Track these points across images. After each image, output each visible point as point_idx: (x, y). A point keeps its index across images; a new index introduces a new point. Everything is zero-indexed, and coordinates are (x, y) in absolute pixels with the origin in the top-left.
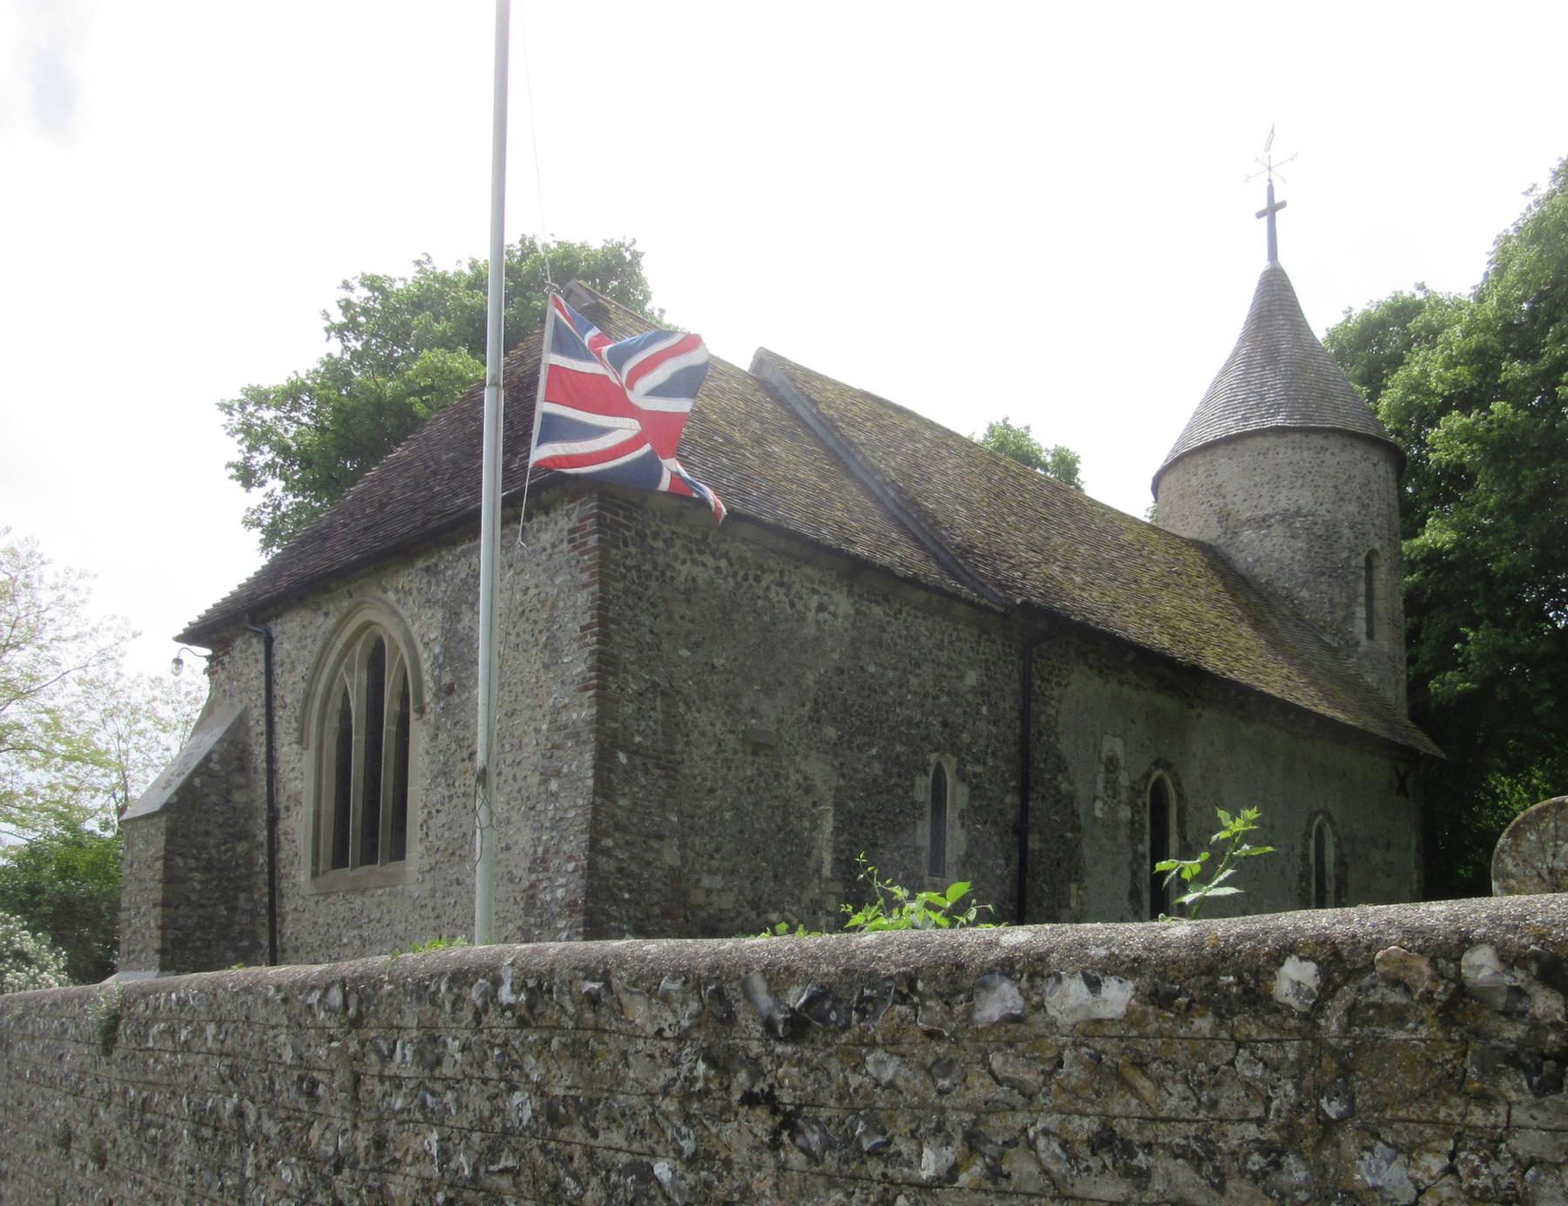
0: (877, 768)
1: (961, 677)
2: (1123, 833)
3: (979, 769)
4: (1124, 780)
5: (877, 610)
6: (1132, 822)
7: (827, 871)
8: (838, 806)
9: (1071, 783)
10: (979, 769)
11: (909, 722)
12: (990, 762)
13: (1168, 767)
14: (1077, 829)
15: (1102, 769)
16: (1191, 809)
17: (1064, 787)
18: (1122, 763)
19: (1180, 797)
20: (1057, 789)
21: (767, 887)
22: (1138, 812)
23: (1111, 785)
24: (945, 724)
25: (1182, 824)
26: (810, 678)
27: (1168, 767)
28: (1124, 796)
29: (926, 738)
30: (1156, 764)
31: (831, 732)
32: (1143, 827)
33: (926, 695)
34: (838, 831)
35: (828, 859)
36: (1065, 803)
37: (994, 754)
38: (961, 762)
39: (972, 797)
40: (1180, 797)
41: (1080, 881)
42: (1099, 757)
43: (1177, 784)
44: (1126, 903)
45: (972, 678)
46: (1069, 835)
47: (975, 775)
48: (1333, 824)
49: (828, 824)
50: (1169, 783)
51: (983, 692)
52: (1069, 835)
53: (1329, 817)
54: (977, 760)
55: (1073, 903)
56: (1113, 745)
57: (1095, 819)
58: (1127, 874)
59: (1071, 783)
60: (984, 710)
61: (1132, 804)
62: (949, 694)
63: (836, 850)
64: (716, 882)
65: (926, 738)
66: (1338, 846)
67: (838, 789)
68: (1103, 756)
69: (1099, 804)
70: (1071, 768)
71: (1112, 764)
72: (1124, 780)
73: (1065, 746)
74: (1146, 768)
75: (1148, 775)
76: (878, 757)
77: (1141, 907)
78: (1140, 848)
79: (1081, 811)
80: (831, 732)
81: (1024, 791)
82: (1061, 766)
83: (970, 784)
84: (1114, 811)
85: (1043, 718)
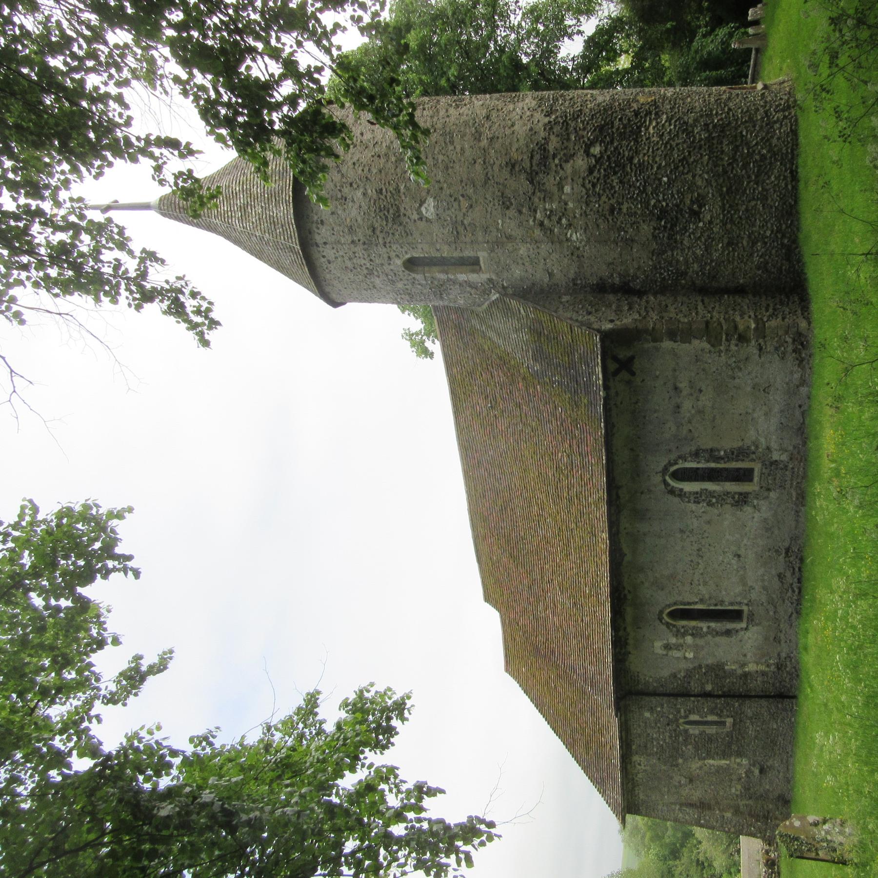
0: (690, 747)
1: (648, 719)
2: (700, 642)
3: (682, 711)
4: (673, 640)
5: (634, 747)
6: (692, 635)
7: (728, 762)
8: (704, 759)
9: (680, 672)
10: (682, 711)
11: (671, 737)
12: (679, 706)
13: (661, 612)
14: (700, 667)
15: (670, 653)
16: (680, 599)
17: (683, 674)
18: (665, 642)
19: (675, 604)
20: (685, 677)
21: (734, 777)
22: (687, 631)
23: (678, 647)
24: (668, 725)
25: (689, 604)
26: (663, 767)
27: (661, 612)
28: (681, 641)
29: (675, 730)
30: (660, 619)
31: (680, 761)
32: (694, 628)
33: (659, 731)
34: (713, 759)
35: (723, 762)
36: (689, 674)
37: (675, 705)
38: (681, 717)
39: (694, 713)
40: (675, 604)
41: (724, 664)
42: (667, 655)
43: (669, 606)
44: (733, 639)
45: (647, 715)
46: (704, 670)
47: (685, 712)
48: (671, 464)
49: (711, 762)
50: (668, 610)
51: (651, 710)
52: (704, 670)
53: (665, 470)
54: (679, 712)
55: (734, 667)
56: (658, 644)
57: (694, 657)
58: (718, 639)
59: (680, 672)
60: (659, 709)
61: (684, 635)
62: (656, 724)
63: (720, 759)
64: (733, 790)
65: (675, 730)
66: (684, 458)
67: (699, 759)
68: (665, 653)
69: (687, 655)
70: (674, 671)
71: (667, 647)
72: (673, 640)
73: (665, 673)
74: (664, 627)
75: (668, 625)
76: (686, 746)
77: (734, 629)
78: (705, 630)
79: (691, 666)
80: (680, 761)
81: (686, 695)
82: (674, 676)
83: (690, 713)
84: (689, 646)
85: (655, 685)
